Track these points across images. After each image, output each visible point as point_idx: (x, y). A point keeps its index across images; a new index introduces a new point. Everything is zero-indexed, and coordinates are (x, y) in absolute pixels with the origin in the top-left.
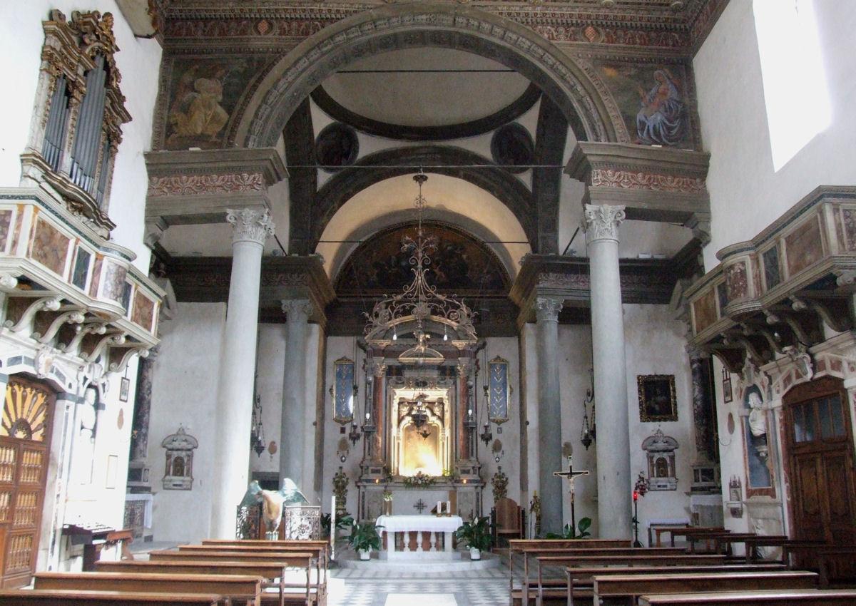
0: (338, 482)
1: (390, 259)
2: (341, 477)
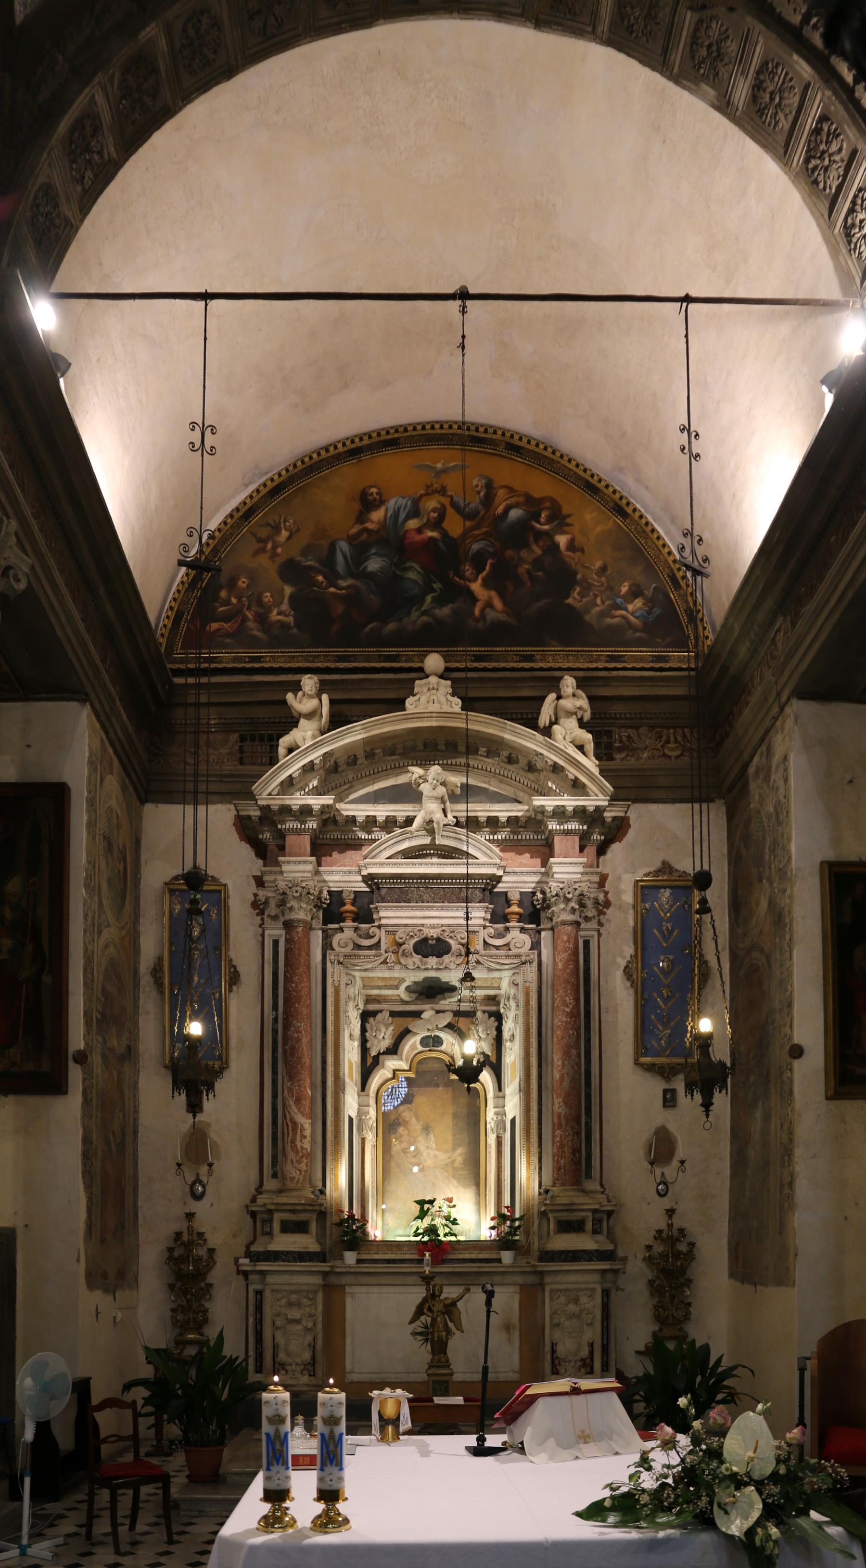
0: (183, 1259)
1: (332, 548)
2: (188, 1246)
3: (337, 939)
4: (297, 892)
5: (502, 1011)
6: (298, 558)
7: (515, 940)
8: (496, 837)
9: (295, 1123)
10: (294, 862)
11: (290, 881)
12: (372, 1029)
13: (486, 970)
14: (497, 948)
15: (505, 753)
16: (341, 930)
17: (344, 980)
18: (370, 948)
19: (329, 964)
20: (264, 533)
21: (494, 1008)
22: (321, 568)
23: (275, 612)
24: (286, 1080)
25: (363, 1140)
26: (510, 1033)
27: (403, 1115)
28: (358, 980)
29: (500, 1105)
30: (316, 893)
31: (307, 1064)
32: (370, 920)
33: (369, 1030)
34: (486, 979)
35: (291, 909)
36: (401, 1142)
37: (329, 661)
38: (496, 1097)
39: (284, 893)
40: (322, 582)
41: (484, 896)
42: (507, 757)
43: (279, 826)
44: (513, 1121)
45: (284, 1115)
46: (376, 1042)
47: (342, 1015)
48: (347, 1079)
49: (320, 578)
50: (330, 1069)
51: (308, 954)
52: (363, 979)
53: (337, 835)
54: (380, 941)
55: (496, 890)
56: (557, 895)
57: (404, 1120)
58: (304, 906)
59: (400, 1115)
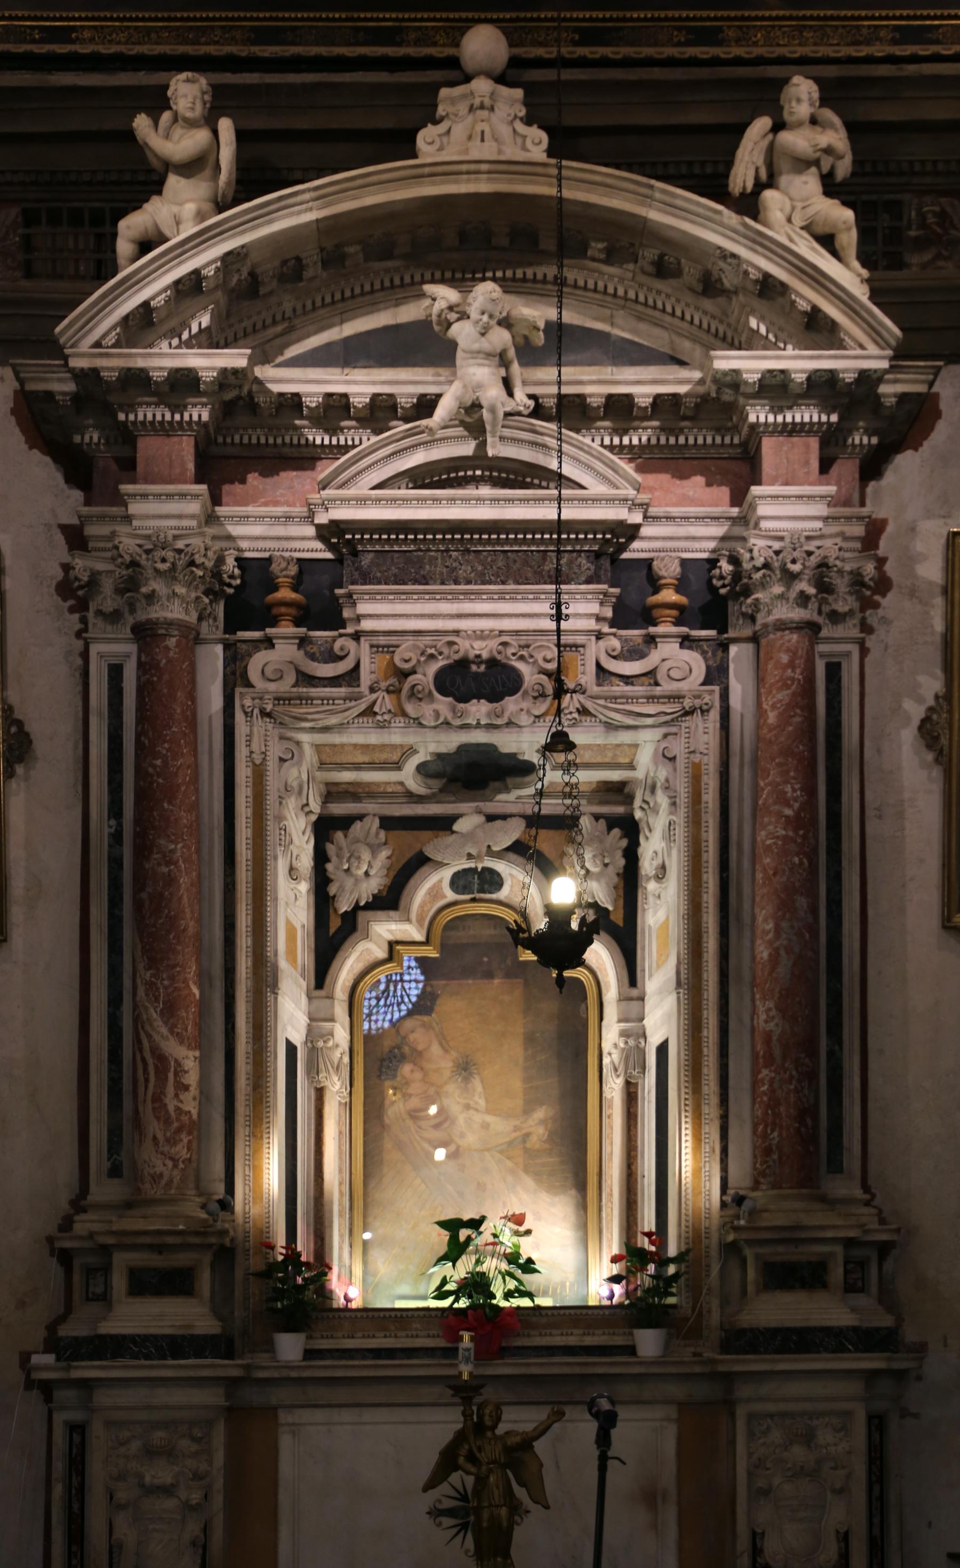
3: (257, 663)
4: (164, 560)
5: (638, 814)
7: (667, 665)
8: (626, 441)
9: (162, 1059)
10: (158, 496)
11: (148, 537)
12: (339, 856)
13: (601, 729)
14: (627, 680)
15: (649, 254)
16: (269, 643)
17: (276, 750)
18: (334, 681)
19: (239, 717)
21: (620, 810)
24: (141, 966)
25: (320, 1094)
26: (658, 861)
27: (412, 1037)
28: (308, 751)
29: (634, 1014)
31: (191, 931)
32: (334, 621)
33: (334, 859)
34: (601, 748)
35: (151, 597)
36: (406, 1096)
38: (623, 998)
39: (134, 564)
41: (598, 568)
42: (653, 263)
44: (662, 1050)
45: (138, 1041)
46: (349, 883)
47: (271, 826)
48: (283, 964)
50: (244, 941)
51: (192, 696)
52: (318, 748)
53: (258, 436)
54: (357, 666)
55: (625, 555)
56: (766, 566)
57: (414, 1050)
58: (181, 590)
59: (404, 1038)
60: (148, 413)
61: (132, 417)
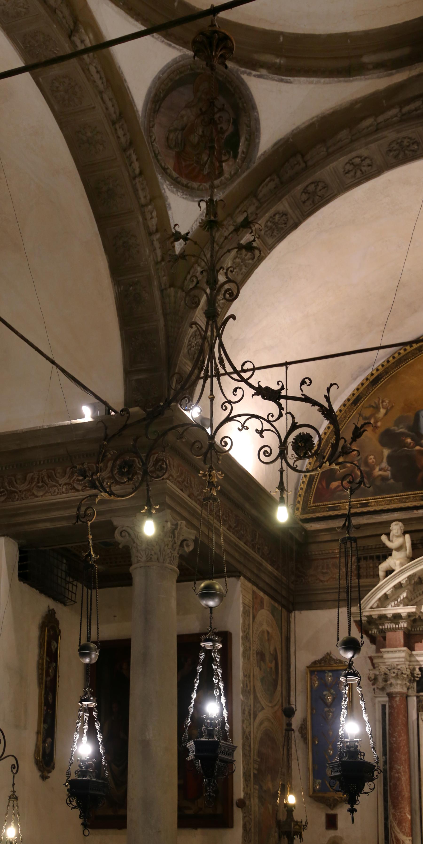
4: (394, 673)
6: (393, 428)
10: (392, 652)
11: (389, 665)
20: (367, 413)
22: (410, 433)
23: (377, 469)
30: (408, 672)
37: (417, 500)
40: (410, 443)
43: (381, 627)
49: (409, 440)
60: (388, 625)
61: (383, 627)
